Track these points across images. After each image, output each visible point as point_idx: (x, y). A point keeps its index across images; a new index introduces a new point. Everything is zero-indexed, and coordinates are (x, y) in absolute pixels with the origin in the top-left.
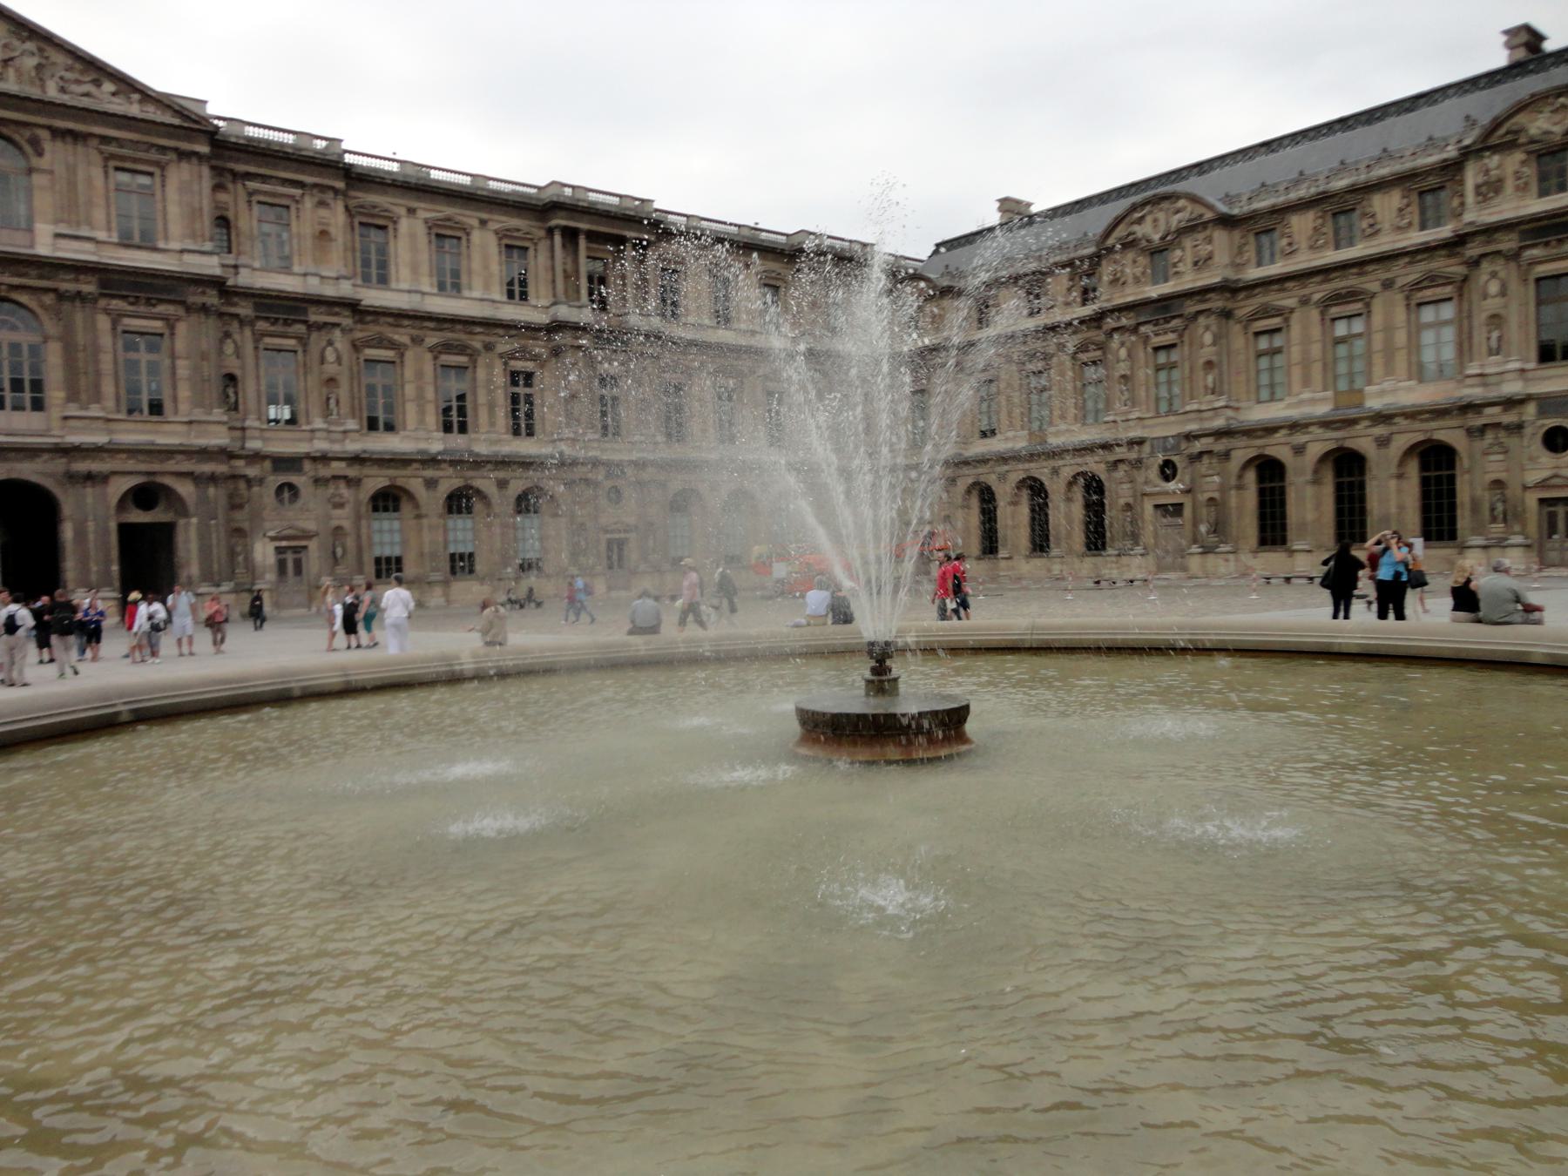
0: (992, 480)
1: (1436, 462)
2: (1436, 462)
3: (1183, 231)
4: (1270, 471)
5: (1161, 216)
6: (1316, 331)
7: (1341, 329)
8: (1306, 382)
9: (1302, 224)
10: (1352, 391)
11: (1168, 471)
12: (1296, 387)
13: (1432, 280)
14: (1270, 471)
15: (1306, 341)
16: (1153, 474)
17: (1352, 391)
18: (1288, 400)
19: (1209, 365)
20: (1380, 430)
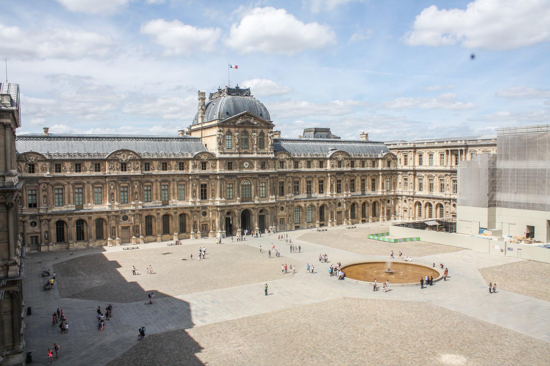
0: (66, 220)
1: (183, 216)
2: (183, 216)
3: (130, 160)
4: (149, 218)
5: (126, 155)
6: (159, 188)
7: (163, 188)
8: (157, 199)
9: (156, 164)
10: (165, 201)
11: (125, 218)
12: (154, 199)
13: (182, 181)
14: (149, 218)
15: (157, 190)
16: (121, 220)
17: (165, 201)
18: (152, 202)
19: (136, 193)
20: (175, 211)
